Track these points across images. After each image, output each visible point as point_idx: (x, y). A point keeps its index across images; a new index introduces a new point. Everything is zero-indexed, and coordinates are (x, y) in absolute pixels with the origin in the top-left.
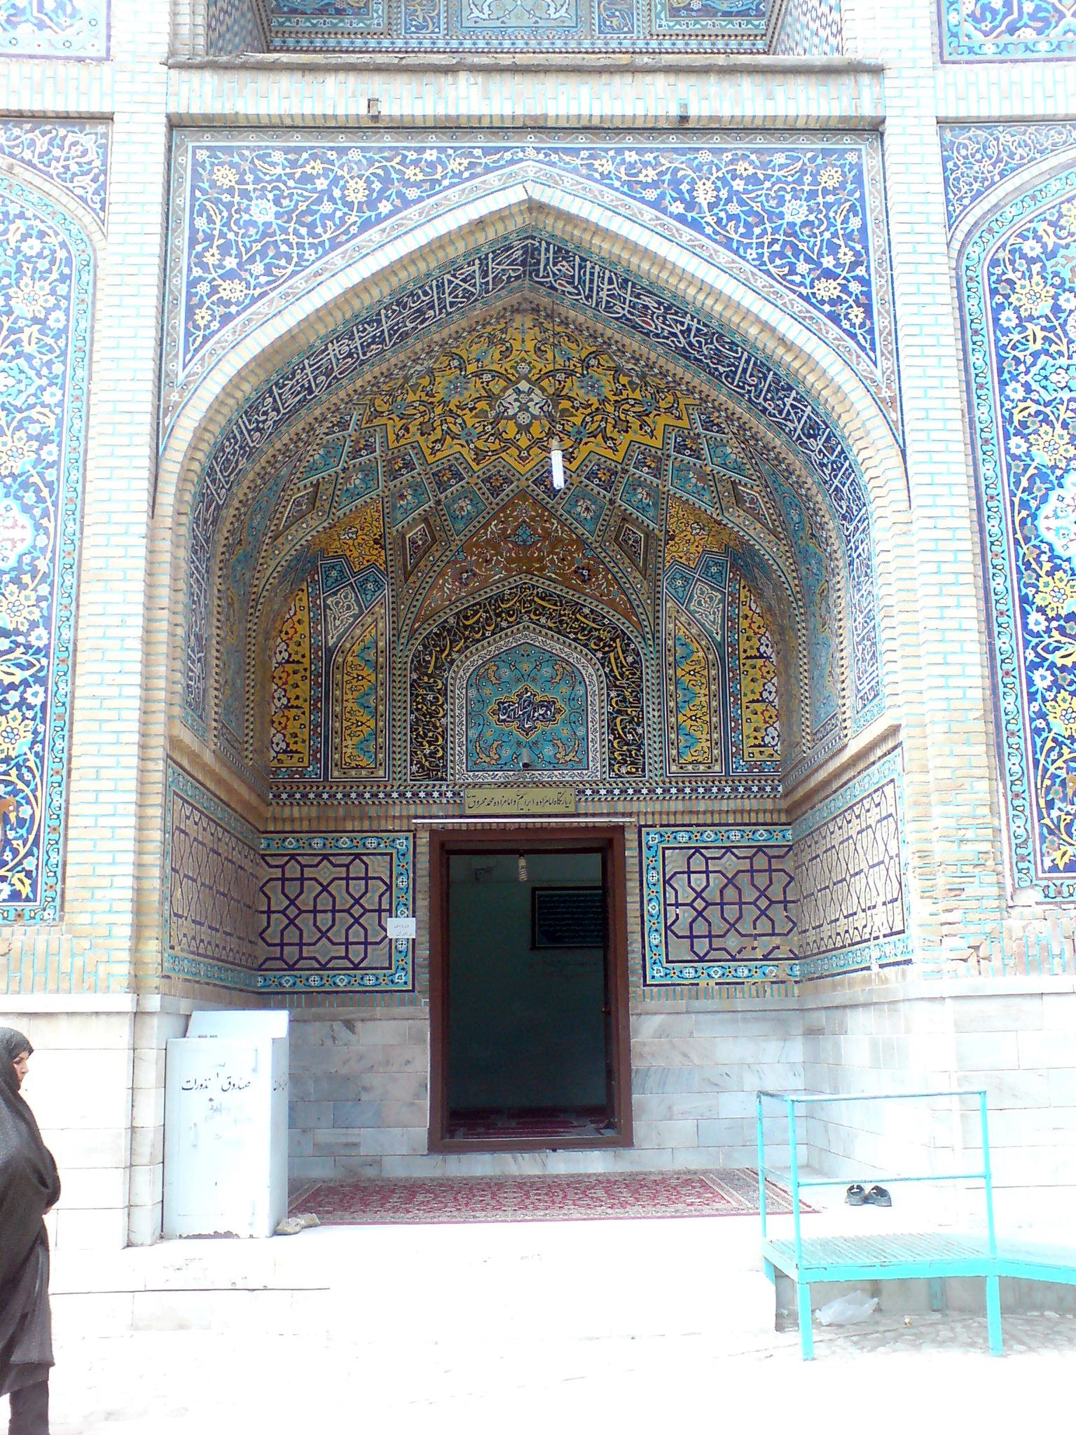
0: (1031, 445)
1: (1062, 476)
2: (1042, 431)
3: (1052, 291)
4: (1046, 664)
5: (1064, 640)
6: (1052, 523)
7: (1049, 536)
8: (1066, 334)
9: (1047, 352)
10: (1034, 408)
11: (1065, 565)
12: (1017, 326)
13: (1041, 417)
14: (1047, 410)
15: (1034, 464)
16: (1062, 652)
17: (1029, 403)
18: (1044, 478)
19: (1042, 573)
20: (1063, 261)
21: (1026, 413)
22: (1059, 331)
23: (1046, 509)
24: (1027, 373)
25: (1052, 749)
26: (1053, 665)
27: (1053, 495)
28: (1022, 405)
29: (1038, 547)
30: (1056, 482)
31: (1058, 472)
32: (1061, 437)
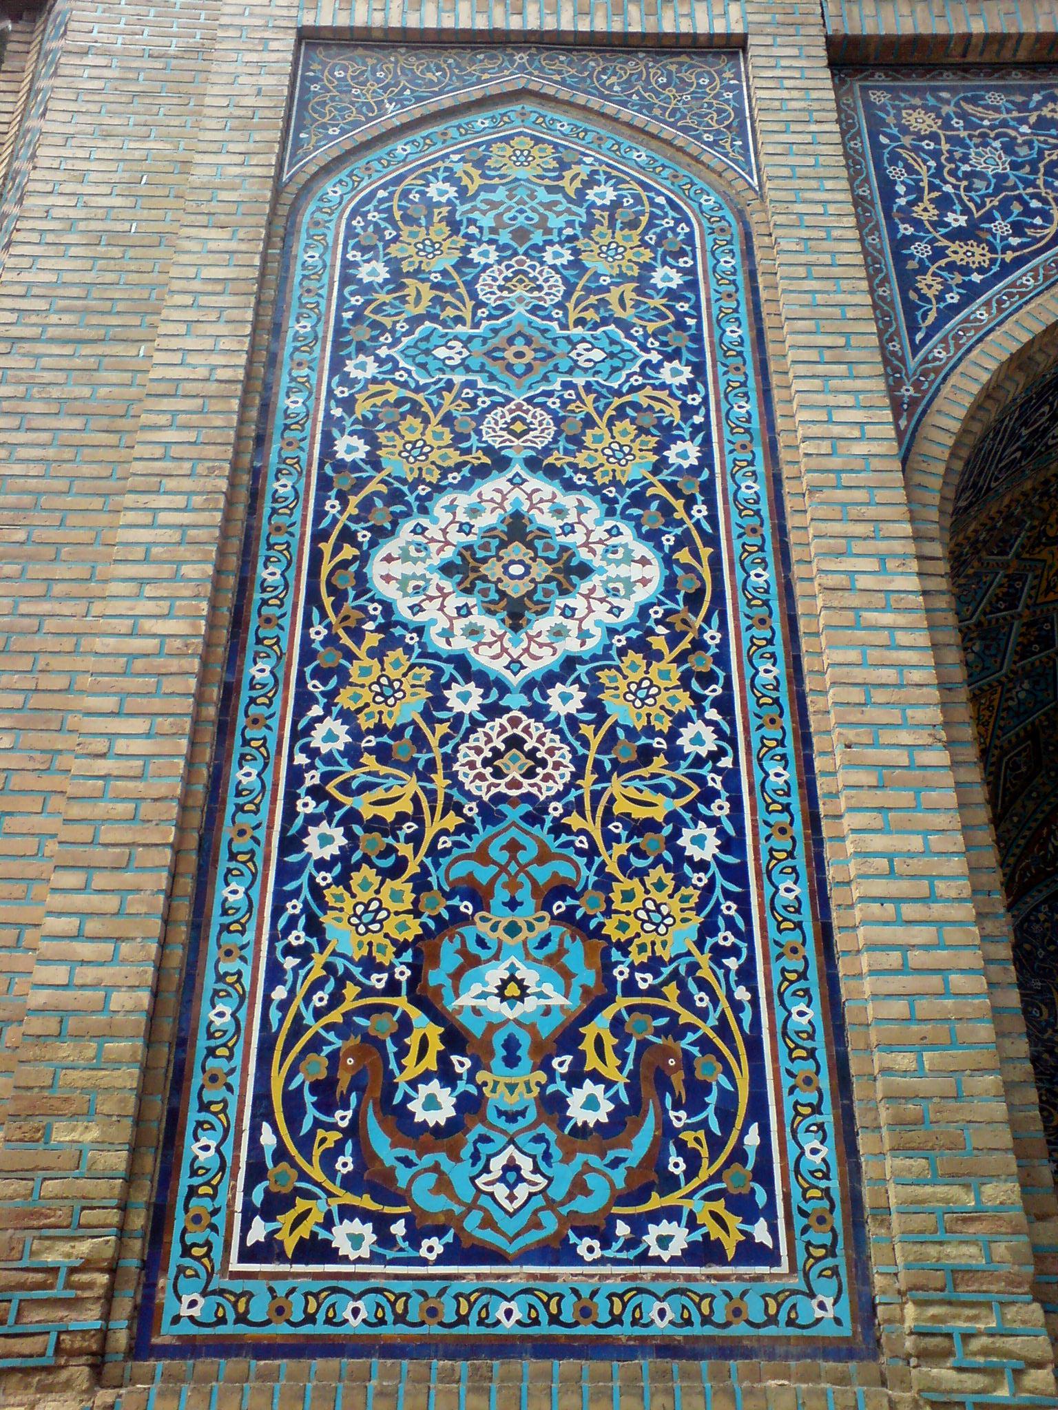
0: (379, 446)
1: (429, 497)
2: (403, 427)
3: (462, 242)
4: (338, 814)
5: (384, 770)
6: (397, 569)
7: (389, 591)
8: (473, 295)
9: (434, 318)
10: (396, 393)
11: (412, 639)
12: (386, 282)
13: (407, 407)
14: (420, 397)
15: (379, 476)
16: (379, 794)
17: (389, 386)
18: (395, 496)
19: (361, 652)
20: (485, 207)
21: (379, 401)
22: (462, 290)
23: (390, 547)
24: (396, 342)
25: (318, 985)
26: (353, 816)
27: (407, 526)
28: (374, 388)
29: (363, 609)
30: (415, 505)
31: (422, 490)
32: (438, 436)
